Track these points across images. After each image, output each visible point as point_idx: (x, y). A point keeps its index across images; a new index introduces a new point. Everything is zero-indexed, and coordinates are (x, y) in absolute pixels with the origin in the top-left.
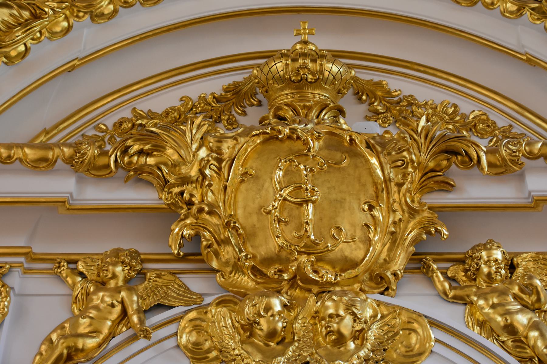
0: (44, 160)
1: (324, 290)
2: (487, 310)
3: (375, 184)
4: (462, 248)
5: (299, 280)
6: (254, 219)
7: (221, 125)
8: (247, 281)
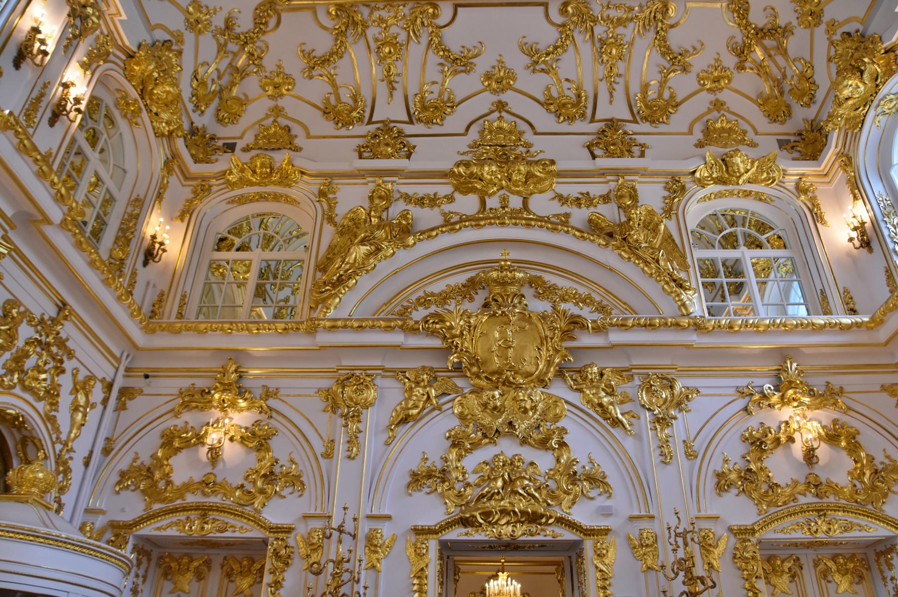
0: (390, 327)
1: (519, 387)
4: (579, 365)
5: (507, 383)
8: (484, 383)
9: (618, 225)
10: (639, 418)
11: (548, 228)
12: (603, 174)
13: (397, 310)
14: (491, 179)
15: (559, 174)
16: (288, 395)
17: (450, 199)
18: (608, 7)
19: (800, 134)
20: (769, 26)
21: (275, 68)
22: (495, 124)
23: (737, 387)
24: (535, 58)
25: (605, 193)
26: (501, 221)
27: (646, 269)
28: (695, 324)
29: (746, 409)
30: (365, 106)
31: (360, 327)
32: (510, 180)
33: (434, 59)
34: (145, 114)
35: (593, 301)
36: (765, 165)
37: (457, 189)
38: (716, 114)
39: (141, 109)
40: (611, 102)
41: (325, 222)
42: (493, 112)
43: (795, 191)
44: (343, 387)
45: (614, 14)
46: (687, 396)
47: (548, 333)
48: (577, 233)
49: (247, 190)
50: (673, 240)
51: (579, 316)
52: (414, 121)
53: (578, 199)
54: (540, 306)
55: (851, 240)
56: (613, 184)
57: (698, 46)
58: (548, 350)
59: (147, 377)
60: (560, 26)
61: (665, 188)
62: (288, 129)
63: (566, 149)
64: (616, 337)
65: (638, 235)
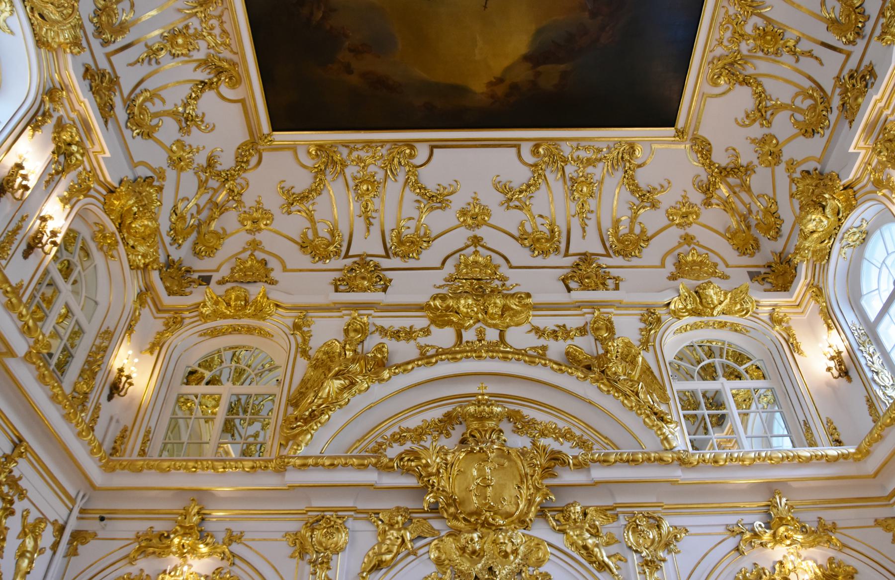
0: (363, 465)
1: (498, 529)
2: (575, 537)
3: (520, 475)
4: (561, 504)
5: (486, 524)
6: (464, 494)
7: (442, 436)
8: (461, 525)
9: (596, 358)
10: (626, 561)
11: (525, 361)
12: (579, 307)
13: (370, 446)
14: (468, 313)
15: (536, 307)
16: (253, 540)
17: (426, 332)
18: (578, 149)
19: (769, 267)
20: (732, 165)
21: (254, 204)
22: (471, 258)
23: (727, 525)
24: (509, 195)
25: (582, 325)
26: (477, 354)
27: (626, 402)
28: (679, 459)
29: (737, 549)
30: (342, 241)
31: (332, 465)
32: (486, 313)
33: (410, 196)
34: (121, 247)
35: (573, 436)
36: (738, 296)
37: (433, 322)
38: (686, 247)
39: (117, 242)
40: (584, 237)
41: (299, 355)
42: (468, 246)
43: (769, 322)
44: (313, 531)
45: (583, 154)
46: (676, 536)
47: (528, 470)
48: (555, 366)
49: (220, 323)
50: (652, 373)
51: (559, 452)
52: (391, 255)
53: (555, 332)
54: (520, 442)
55: (829, 369)
56: (589, 317)
57: (665, 184)
58: (528, 488)
59: (102, 519)
60: (532, 166)
61: (641, 320)
62: (265, 263)
63: (542, 282)
64: (599, 473)
65: (617, 368)
